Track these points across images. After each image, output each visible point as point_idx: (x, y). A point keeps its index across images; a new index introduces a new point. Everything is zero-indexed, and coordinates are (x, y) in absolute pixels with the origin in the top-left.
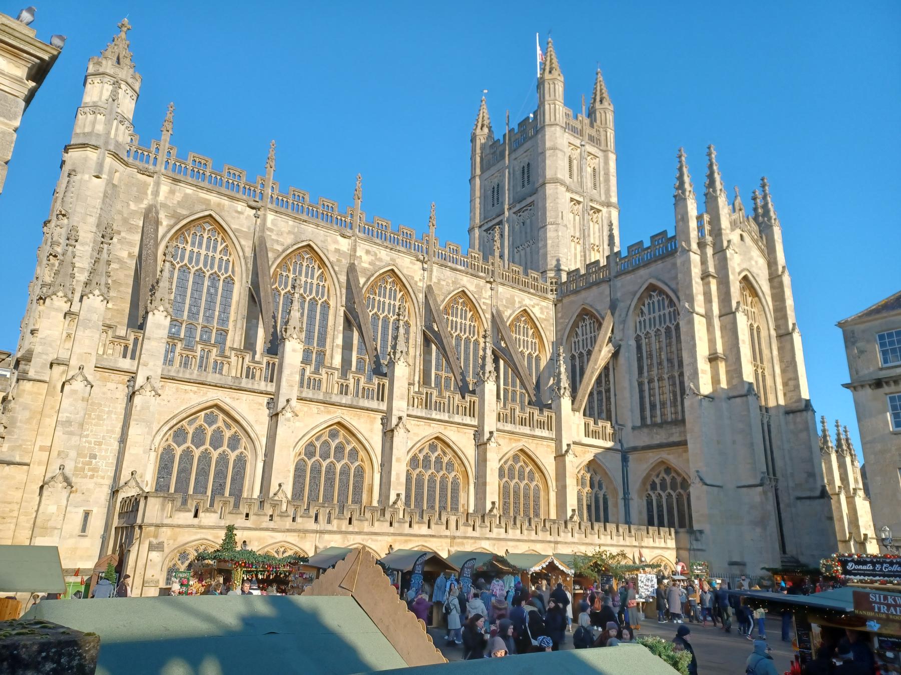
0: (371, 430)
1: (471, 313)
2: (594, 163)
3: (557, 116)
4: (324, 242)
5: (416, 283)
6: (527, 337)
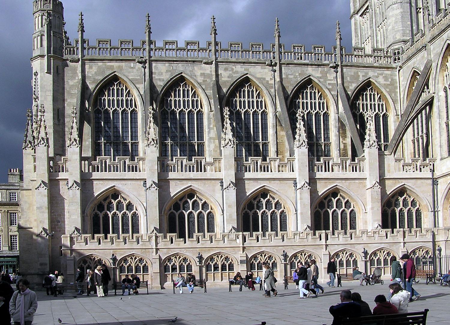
0: (214, 191)
5: (268, 81)
6: (374, 101)
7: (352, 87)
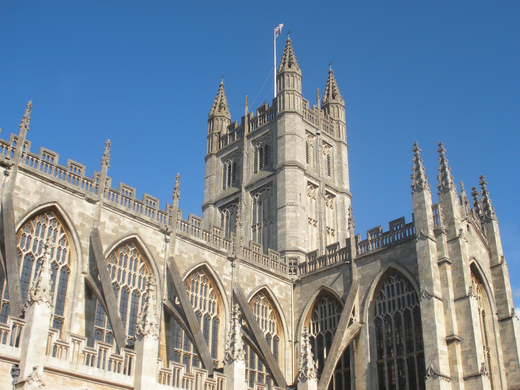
1: (212, 289)
3: (296, 105)
4: (69, 204)
5: (158, 253)
6: (266, 316)
7: (248, 291)
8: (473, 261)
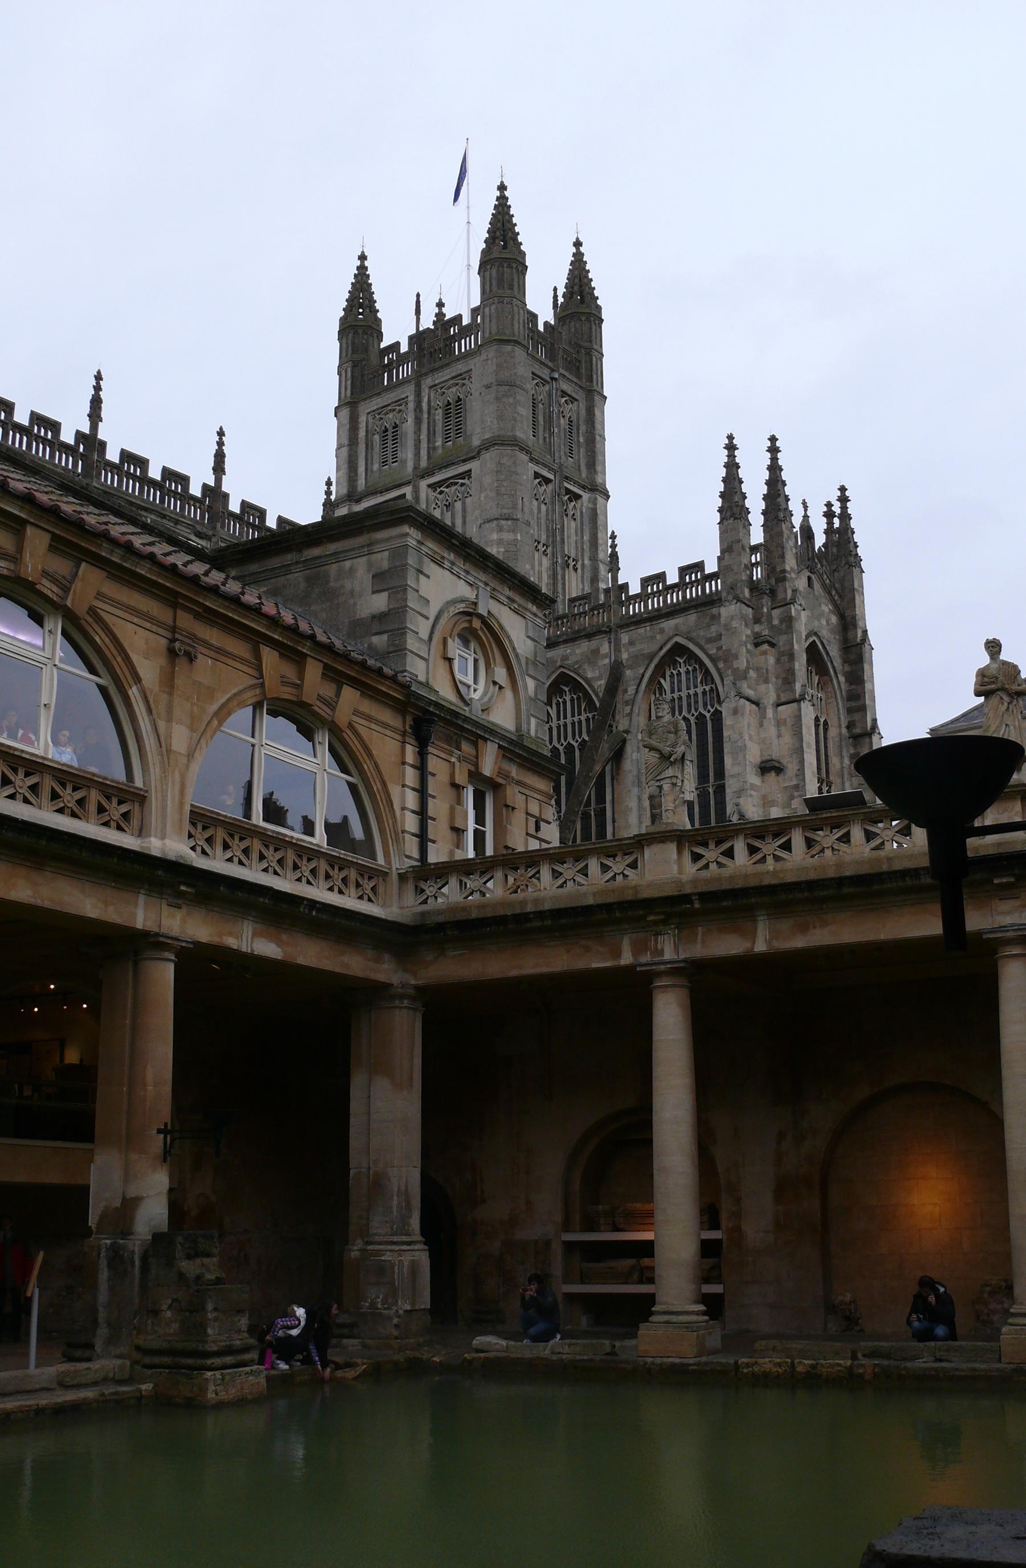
2: (570, 409)
8: (811, 640)
